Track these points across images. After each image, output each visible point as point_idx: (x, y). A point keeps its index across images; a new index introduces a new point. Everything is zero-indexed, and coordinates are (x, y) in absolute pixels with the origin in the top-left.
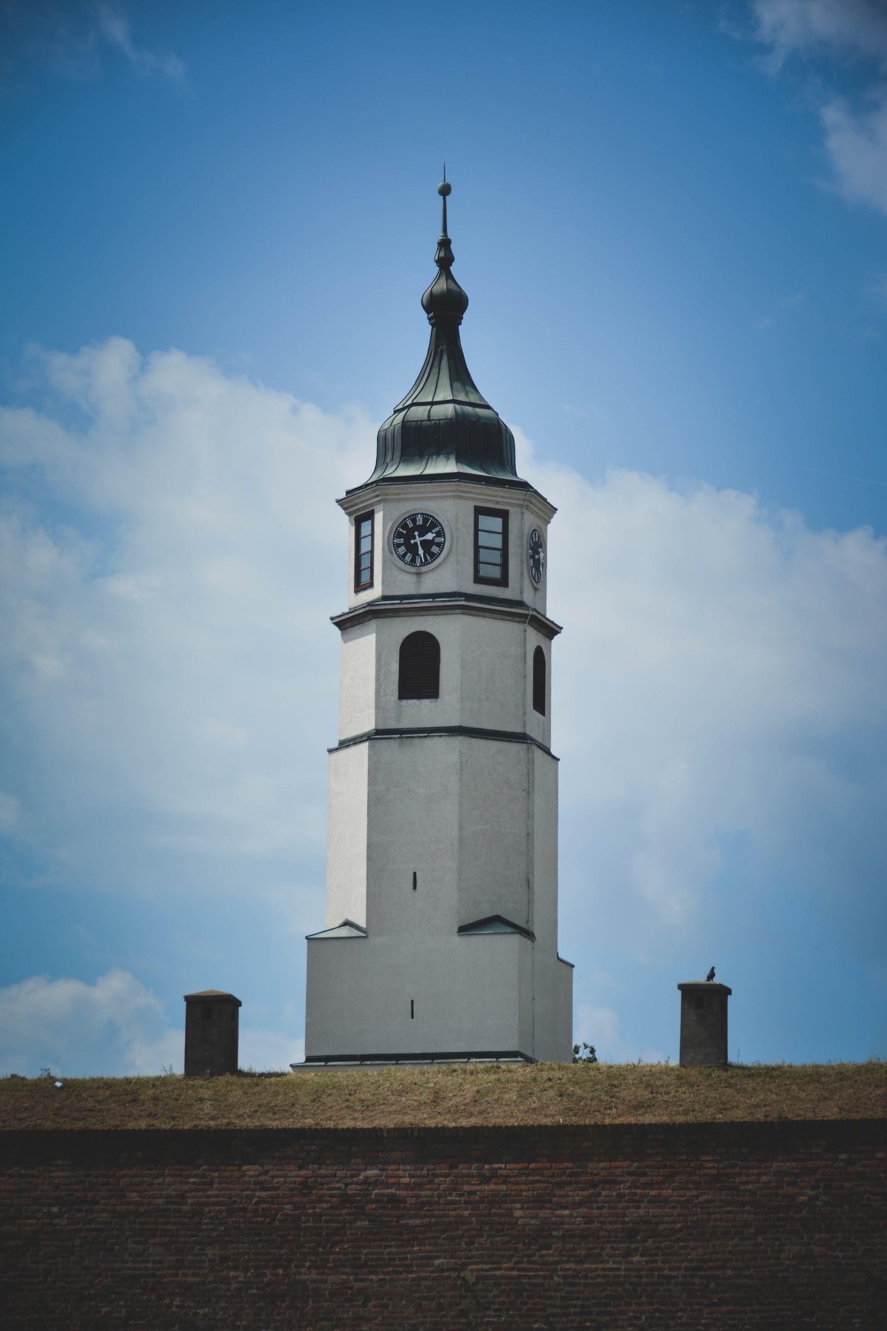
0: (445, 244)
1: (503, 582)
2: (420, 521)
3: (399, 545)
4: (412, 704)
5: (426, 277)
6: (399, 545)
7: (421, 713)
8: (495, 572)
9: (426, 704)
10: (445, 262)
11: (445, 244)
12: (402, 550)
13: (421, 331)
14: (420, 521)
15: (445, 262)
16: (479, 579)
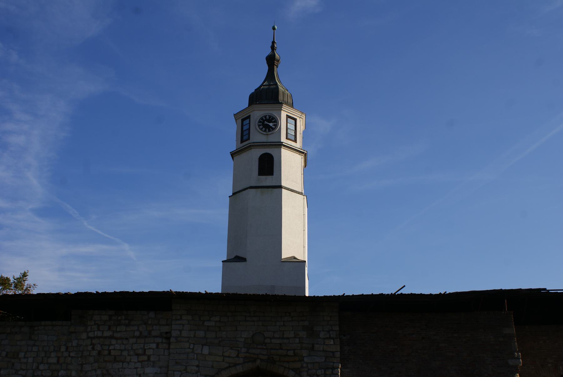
0: (273, 42)
1: (295, 141)
2: (268, 117)
3: (260, 125)
4: (264, 177)
5: (269, 51)
6: (260, 125)
7: (268, 181)
8: (293, 138)
9: (269, 177)
10: (273, 48)
11: (273, 42)
12: (261, 127)
13: (266, 68)
14: (268, 117)
15: (273, 48)
16: (287, 138)
